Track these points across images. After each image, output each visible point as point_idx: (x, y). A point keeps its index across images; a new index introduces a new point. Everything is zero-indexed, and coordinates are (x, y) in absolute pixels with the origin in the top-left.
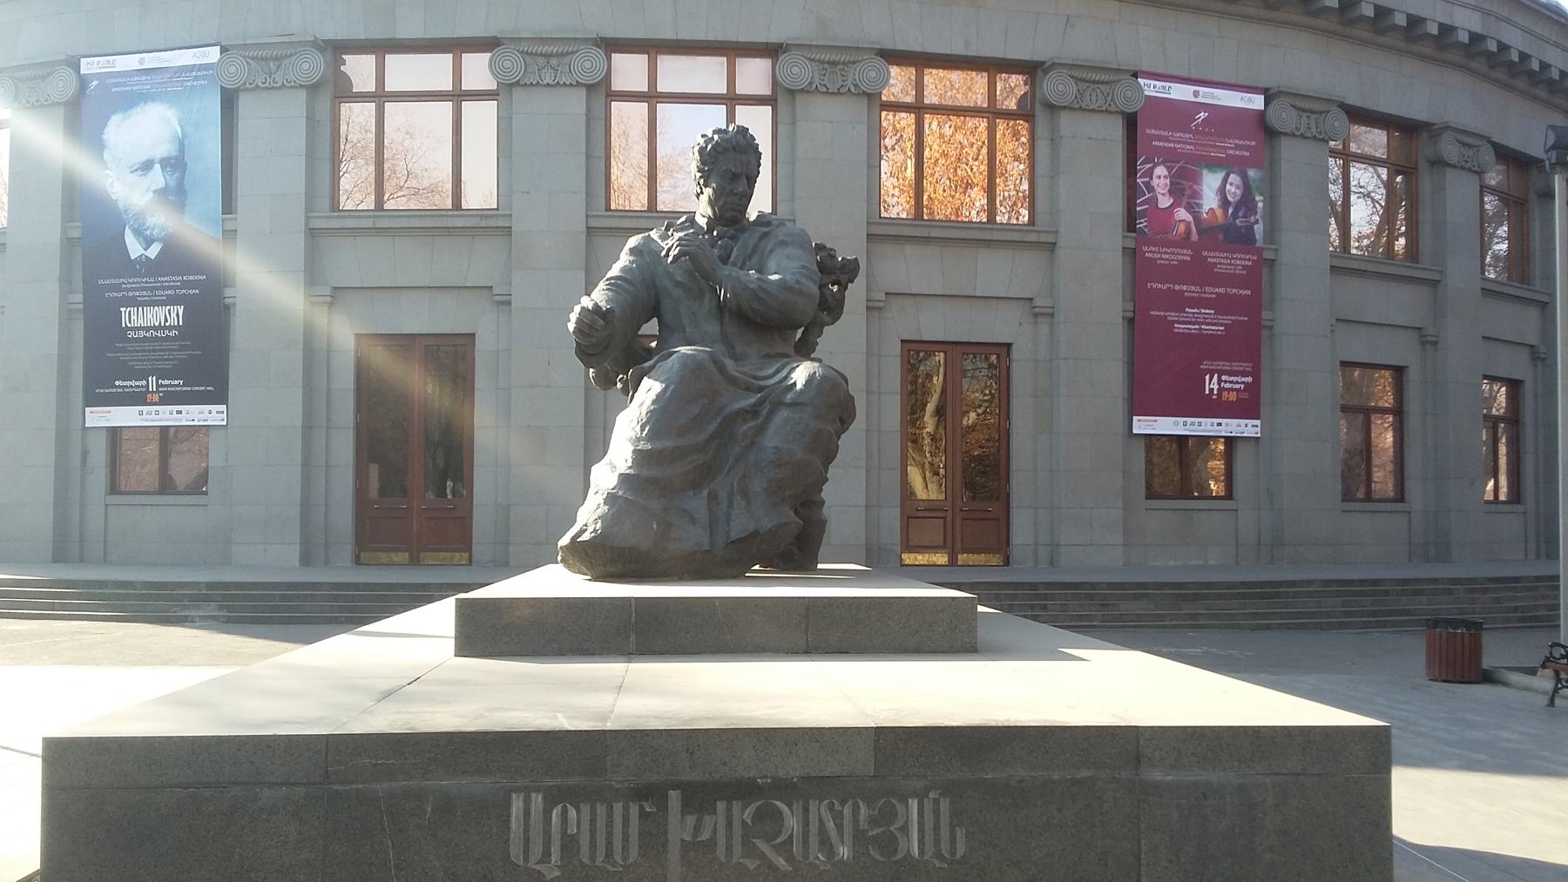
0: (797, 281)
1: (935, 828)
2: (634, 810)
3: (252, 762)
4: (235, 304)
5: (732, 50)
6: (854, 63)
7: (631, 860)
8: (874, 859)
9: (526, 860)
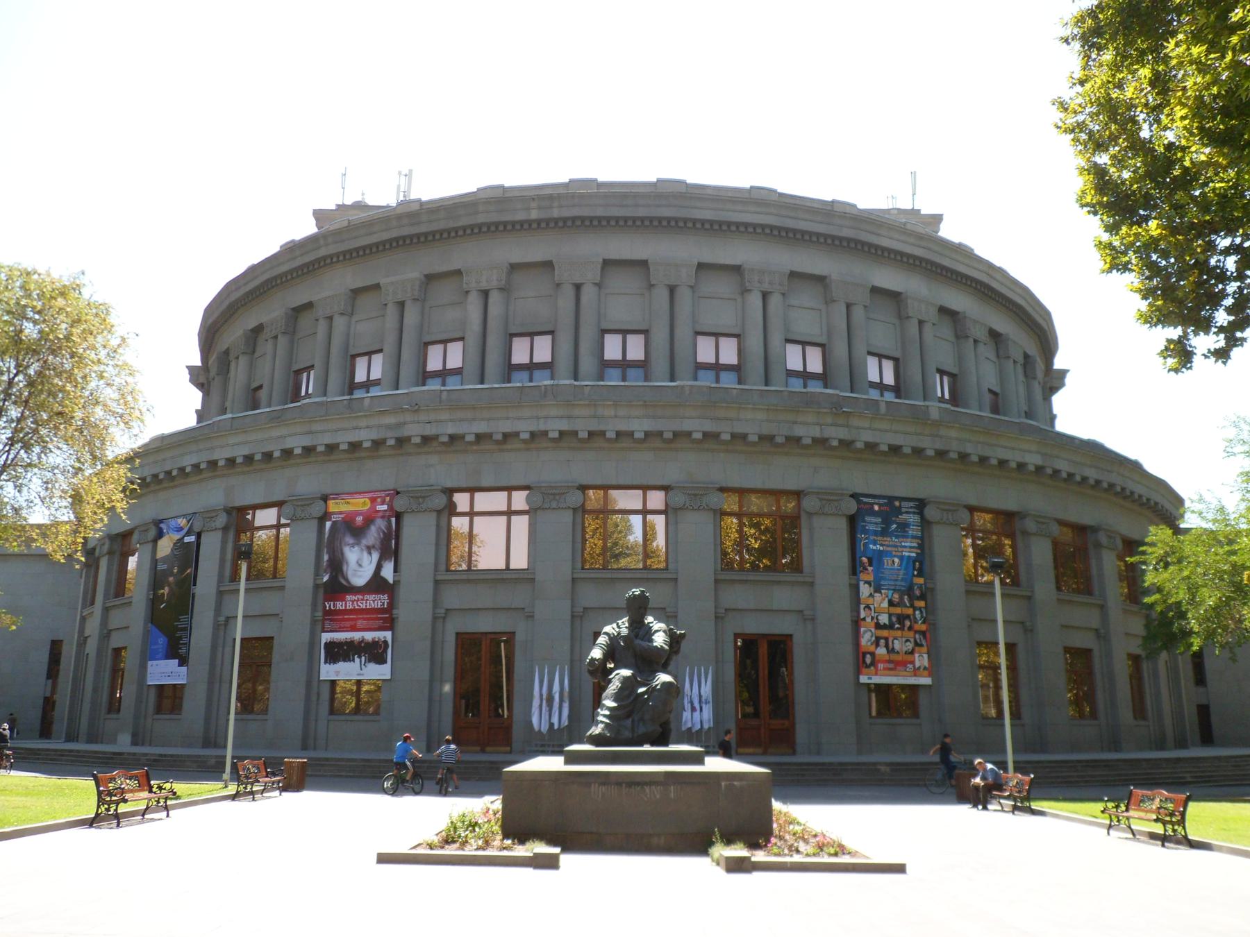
5: (645, 488)
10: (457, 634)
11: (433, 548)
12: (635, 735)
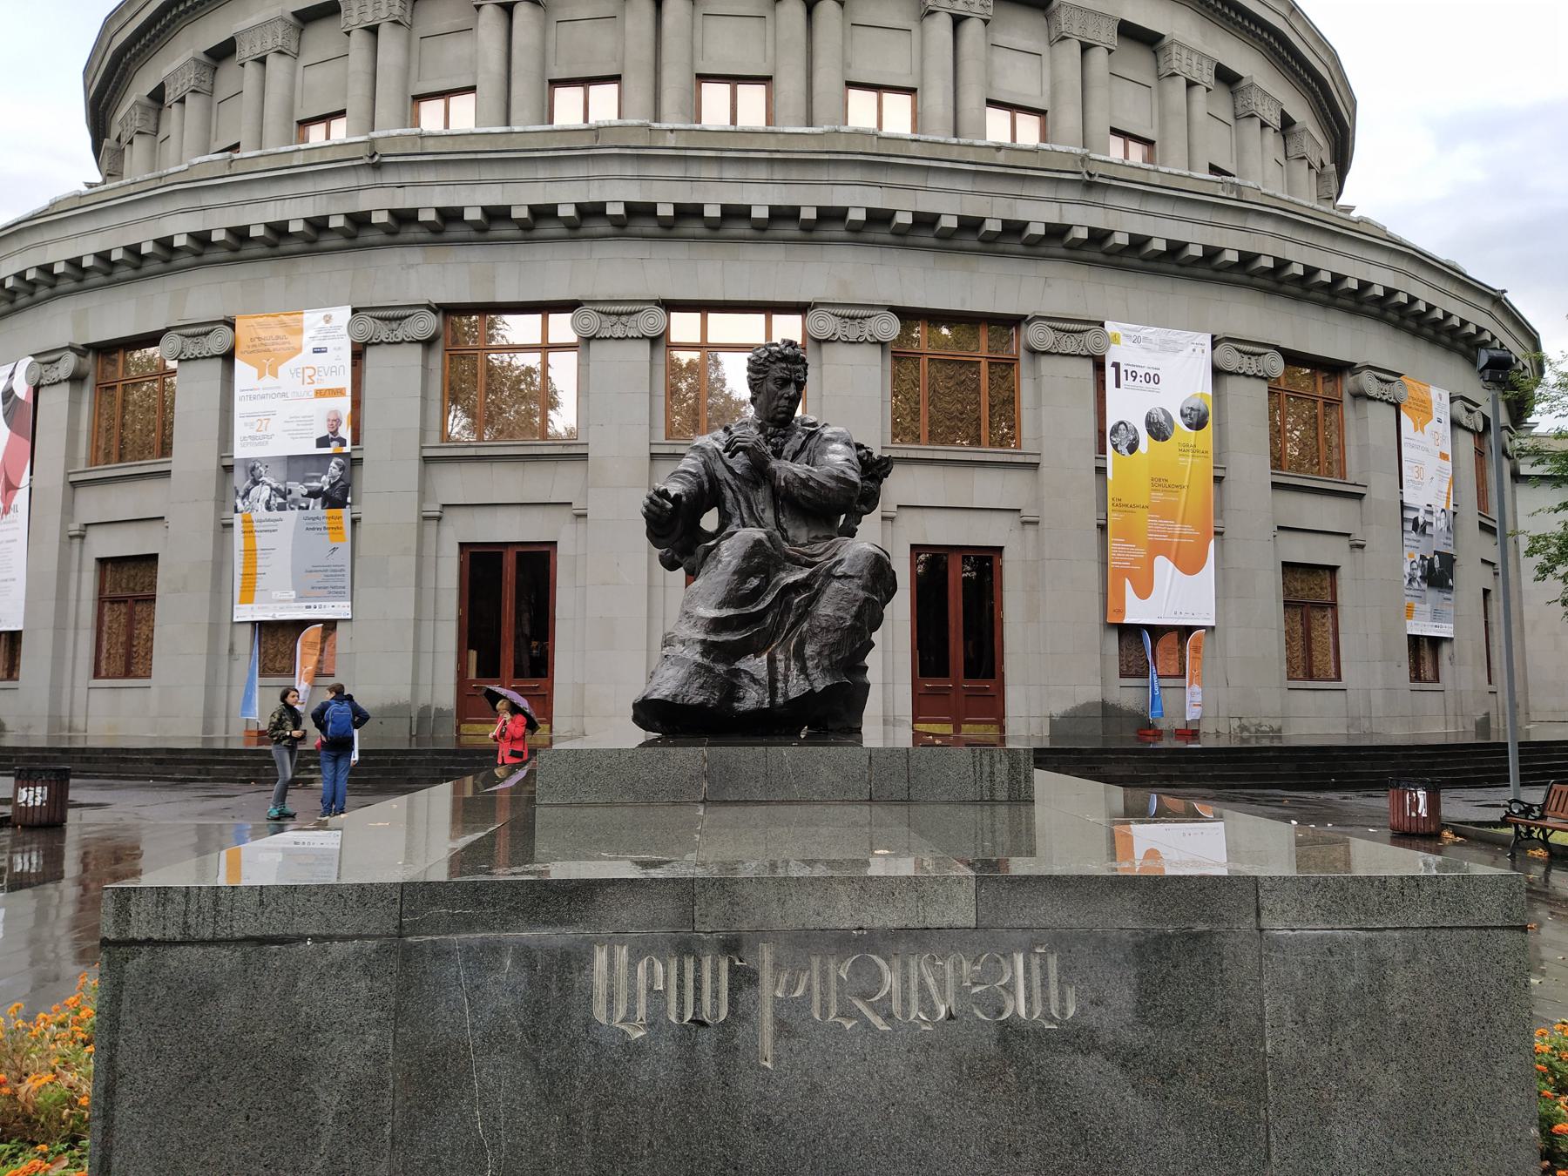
0: (843, 472)
1: (1042, 985)
2: (724, 965)
3: (322, 913)
4: (360, 519)
6: (869, 317)
7: (722, 1018)
8: (979, 1020)
9: (610, 1018)
10: (462, 545)
11: (418, 402)
12: (780, 700)
